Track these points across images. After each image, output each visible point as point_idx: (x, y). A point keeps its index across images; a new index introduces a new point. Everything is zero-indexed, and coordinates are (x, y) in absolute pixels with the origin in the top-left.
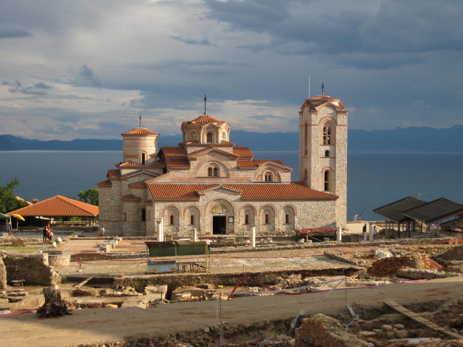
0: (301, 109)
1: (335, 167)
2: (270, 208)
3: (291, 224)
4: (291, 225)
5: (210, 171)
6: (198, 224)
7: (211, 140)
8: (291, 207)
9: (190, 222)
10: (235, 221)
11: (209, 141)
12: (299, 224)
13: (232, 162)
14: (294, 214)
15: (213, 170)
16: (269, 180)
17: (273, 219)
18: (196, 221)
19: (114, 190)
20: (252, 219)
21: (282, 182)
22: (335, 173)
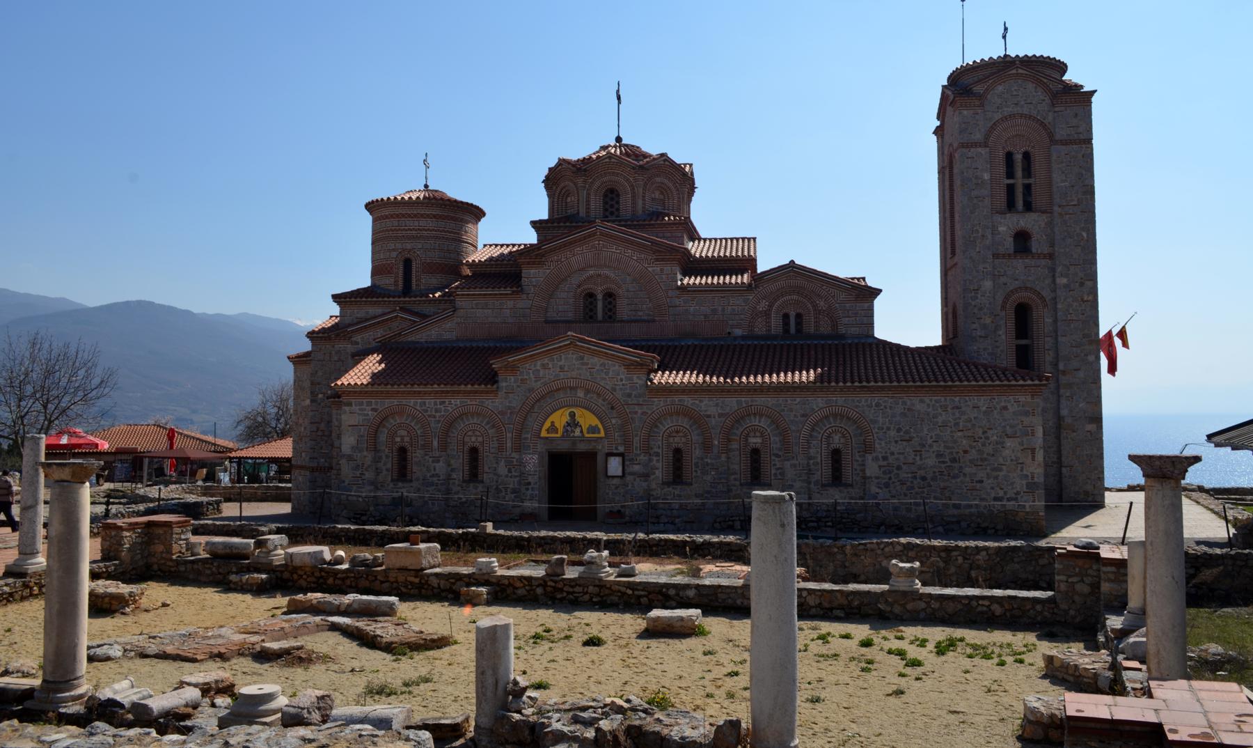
0: (938, 119)
1: (1054, 291)
2: (764, 423)
3: (851, 485)
4: (850, 490)
5: (591, 303)
6: (495, 478)
7: (618, 210)
8: (848, 418)
9: (466, 473)
10: (628, 470)
11: (612, 213)
12: (887, 485)
13: (661, 270)
14: (867, 448)
15: (600, 297)
16: (799, 331)
17: (778, 466)
18: (486, 469)
19: (317, 372)
20: (696, 464)
21: (843, 337)
22: (1055, 310)
